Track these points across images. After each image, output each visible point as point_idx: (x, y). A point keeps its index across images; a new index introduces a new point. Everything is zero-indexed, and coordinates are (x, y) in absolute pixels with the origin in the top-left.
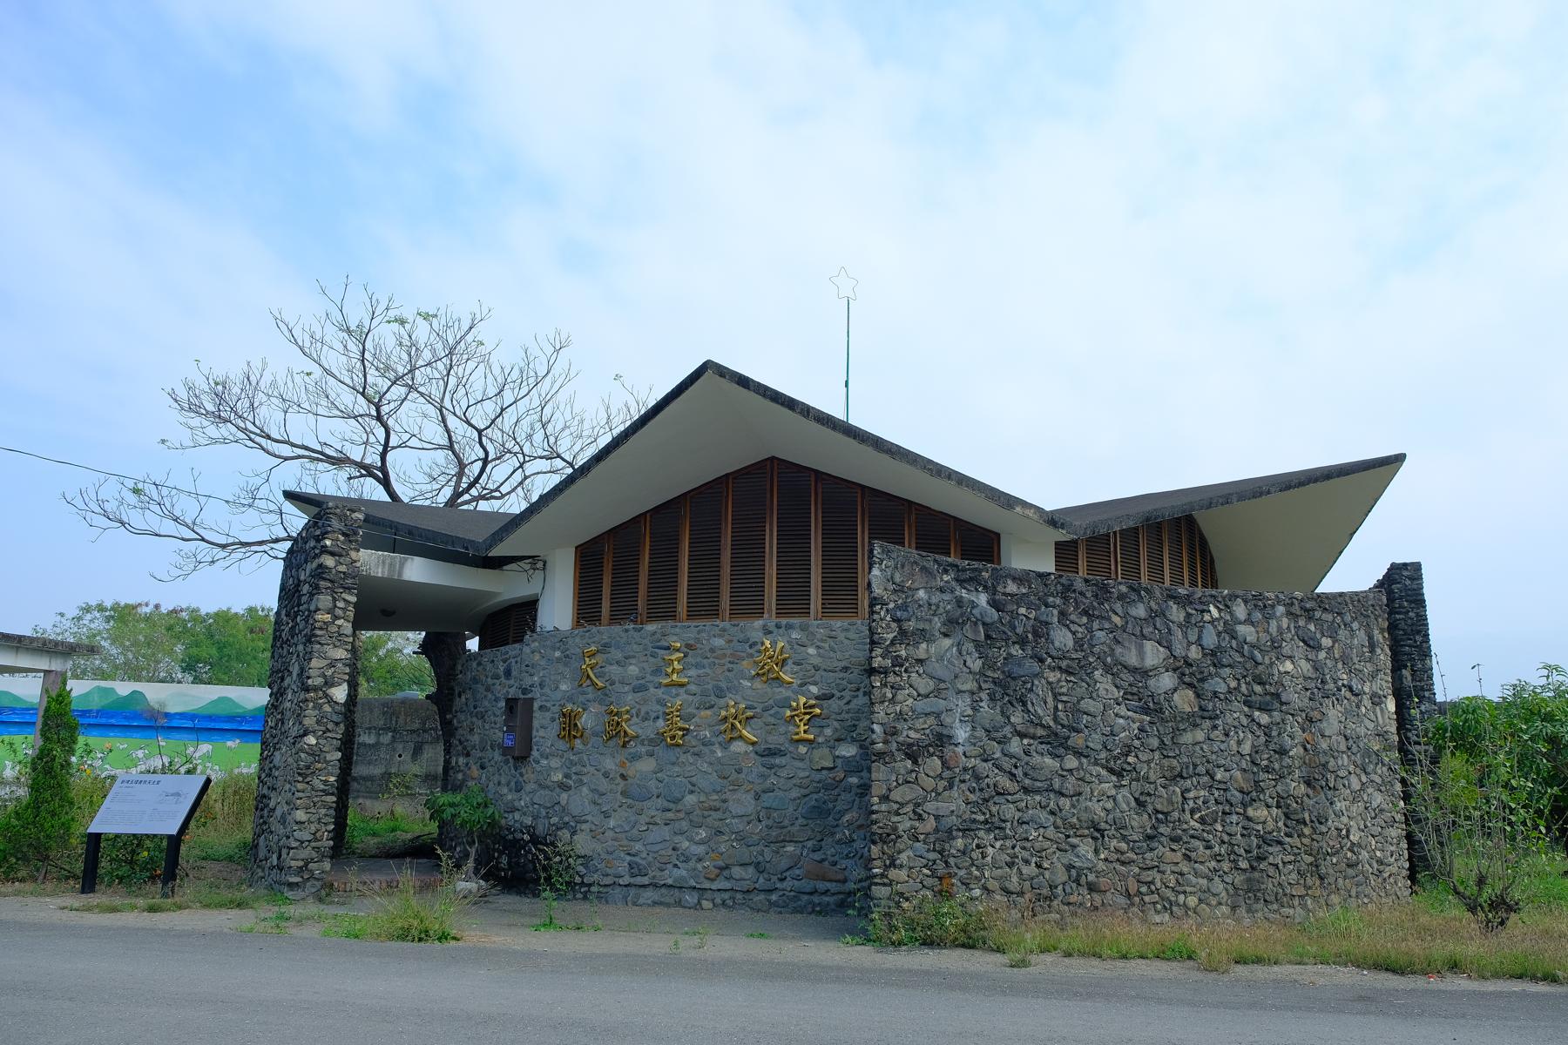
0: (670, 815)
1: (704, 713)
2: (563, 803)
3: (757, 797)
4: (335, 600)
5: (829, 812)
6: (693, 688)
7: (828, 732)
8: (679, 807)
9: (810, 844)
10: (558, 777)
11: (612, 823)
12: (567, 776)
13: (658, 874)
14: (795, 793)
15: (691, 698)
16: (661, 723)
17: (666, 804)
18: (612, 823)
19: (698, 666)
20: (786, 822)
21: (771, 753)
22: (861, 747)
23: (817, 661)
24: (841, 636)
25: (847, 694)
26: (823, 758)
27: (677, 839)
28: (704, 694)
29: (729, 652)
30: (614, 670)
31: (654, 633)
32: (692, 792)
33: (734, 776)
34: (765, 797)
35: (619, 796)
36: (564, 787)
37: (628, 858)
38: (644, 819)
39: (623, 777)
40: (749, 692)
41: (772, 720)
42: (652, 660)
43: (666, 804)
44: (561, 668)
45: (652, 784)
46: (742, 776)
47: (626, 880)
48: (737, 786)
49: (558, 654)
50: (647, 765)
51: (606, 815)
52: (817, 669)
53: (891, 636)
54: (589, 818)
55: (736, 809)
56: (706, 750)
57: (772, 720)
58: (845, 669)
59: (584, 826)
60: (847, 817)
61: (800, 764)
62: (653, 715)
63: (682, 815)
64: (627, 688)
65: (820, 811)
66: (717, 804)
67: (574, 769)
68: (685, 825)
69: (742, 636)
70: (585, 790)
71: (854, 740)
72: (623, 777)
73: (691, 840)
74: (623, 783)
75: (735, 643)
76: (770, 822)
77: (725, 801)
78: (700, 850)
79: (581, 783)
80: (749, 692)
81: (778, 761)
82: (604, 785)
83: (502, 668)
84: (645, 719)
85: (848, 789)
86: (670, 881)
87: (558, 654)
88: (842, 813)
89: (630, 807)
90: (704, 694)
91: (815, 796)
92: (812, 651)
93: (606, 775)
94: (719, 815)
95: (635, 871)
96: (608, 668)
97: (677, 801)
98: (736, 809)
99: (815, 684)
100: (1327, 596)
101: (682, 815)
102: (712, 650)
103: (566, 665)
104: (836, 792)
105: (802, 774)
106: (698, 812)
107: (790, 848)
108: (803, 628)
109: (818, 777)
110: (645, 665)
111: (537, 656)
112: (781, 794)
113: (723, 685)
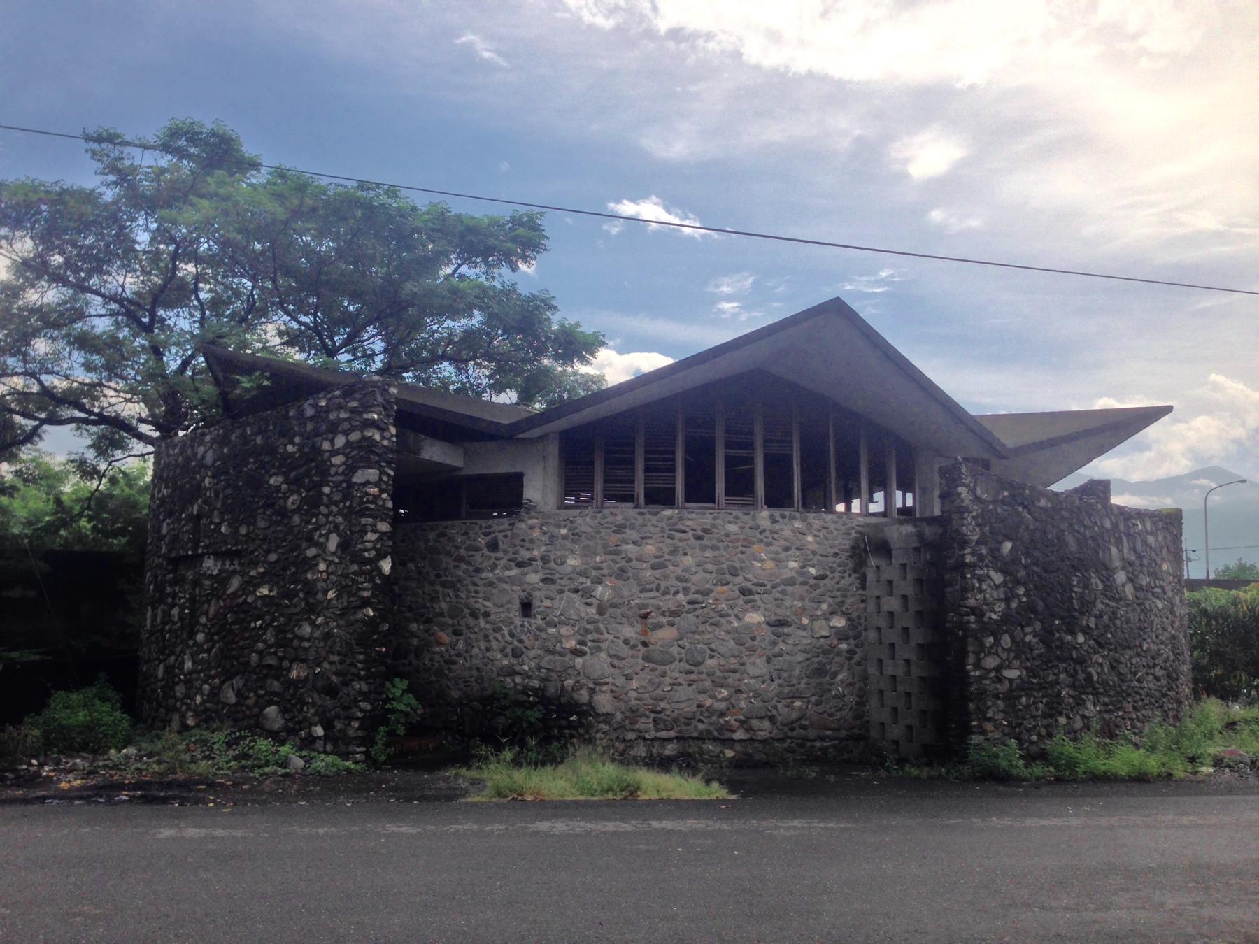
0: (692, 677)
1: (720, 588)
2: (579, 667)
3: (769, 661)
4: (381, 473)
5: (826, 673)
6: (710, 567)
7: (824, 606)
8: (701, 668)
9: (813, 699)
10: (572, 643)
11: (634, 684)
12: (582, 643)
13: (684, 728)
14: (800, 657)
15: (708, 576)
16: (681, 596)
17: (688, 667)
18: (634, 684)
19: (713, 548)
20: (794, 682)
21: (781, 623)
22: (849, 619)
23: (815, 547)
24: (832, 527)
25: (837, 574)
26: (822, 629)
27: (701, 697)
28: (721, 572)
29: (741, 537)
30: (630, 549)
31: (671, 518)
32: (712, 657)
33: (749, 643)
34: (775, 660)
35: (641, 661)
36: (576, 653)
37: (652, 715)
38: (668, 680)
39: (645, 644)
40: (760, 572)
41: (779, 595)
42: (667, 540)
43: (688, 667)
44: (568, 544)
45: (675, 650)
46: (756, 643)
47: (653, 734)
48: (752, 650)
49: (564, 531)
50: (667, 634)
51: (628, 678)
52: (814, 553)
53: (976, 538)
54: (610, 680)
55: (753, 671)
56: (723, 621)
57: (779, 595)
58: (836, 555)
59: (604, 688)
60: (840, 677)
61: (804, 634)
62: (673, 590)
63: (704, 676)
64: (645, 565)
65: (820, 671)
66: (737, 666)
67: (589, 637)
68: (708, 684)
69: (752, 524)
70: (603, 655)
71: (843, 614)
72: (645, 644)
73: (713, 697)
74: (643, 650)
75: (747, 529)
76: (781, 681)
77: (742, 664)
78: (723, 706)
79: (599, 649)
80: (760, 572)
81: (786, 630)
82: (625, 651)
83: (482, 541)
84: (666, 593)
85: (839, 654)
86: (695, 734)
87: (564, 531)
88: (835, 674)
89: (653, 670)
90: (721, 572)
91: (816, 660)
92: (810, 538)
93: (626, 642)
94: (738, 676)
95: (661, 726)
96: (624, 547)
97: (697, 664)
98: (753, 671)
99: (813, 566)
100: (1056, 494)
101: (704, 676)
102: (727, 535)
103: (574, 542)
104: (831, 656)
105: (805, 641)
106: (718, 673)
107: (798, 703)
108: (804, 520)
109: (819, 644)
110: (661, 545)
111: (536, 533)
112: (788, 657)
113: (737, 565)
